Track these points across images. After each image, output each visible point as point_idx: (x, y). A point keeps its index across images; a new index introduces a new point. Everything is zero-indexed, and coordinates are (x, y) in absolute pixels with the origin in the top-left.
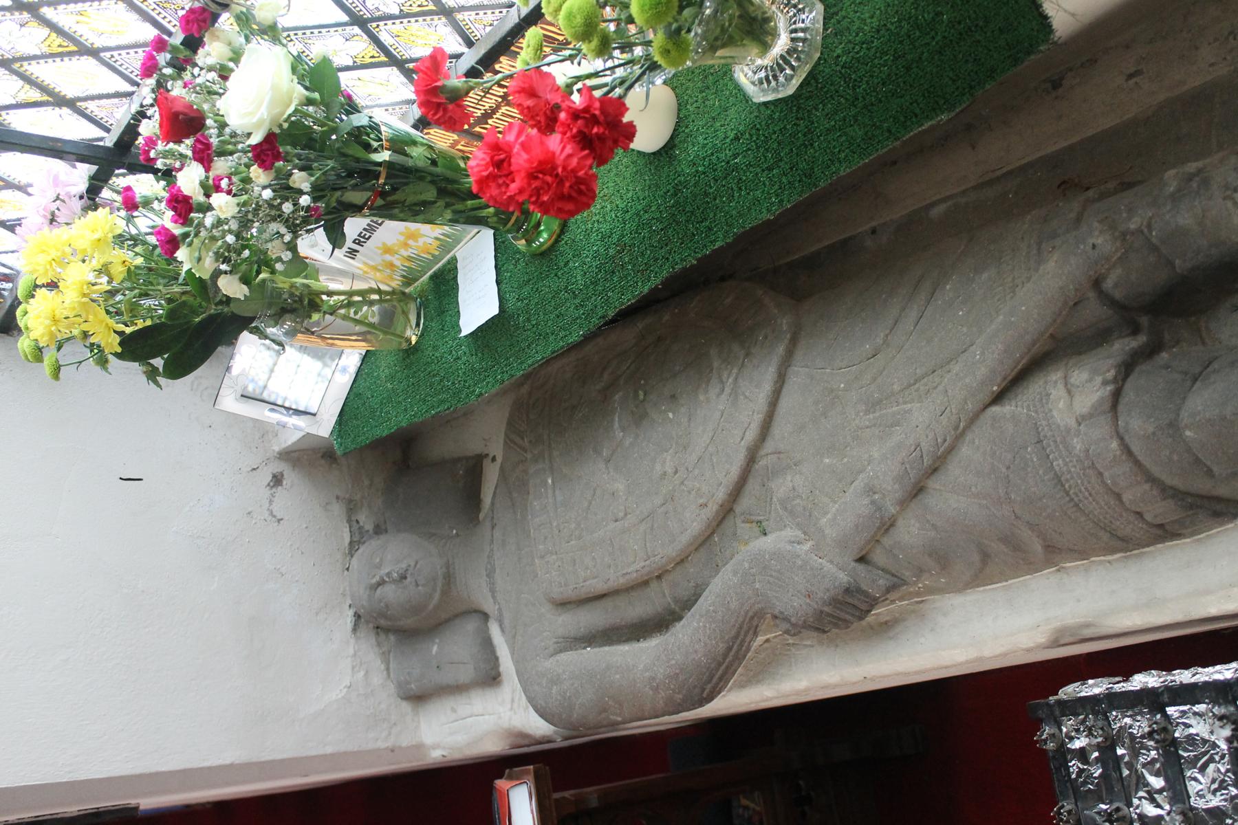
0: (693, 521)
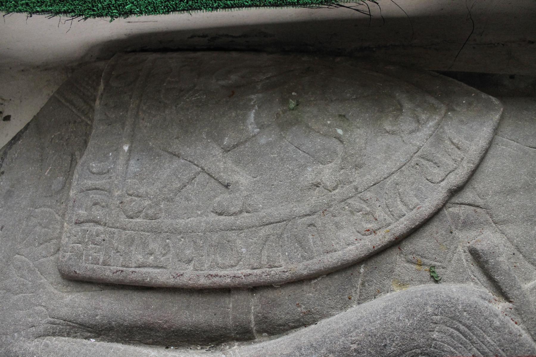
0: (349, 243)
